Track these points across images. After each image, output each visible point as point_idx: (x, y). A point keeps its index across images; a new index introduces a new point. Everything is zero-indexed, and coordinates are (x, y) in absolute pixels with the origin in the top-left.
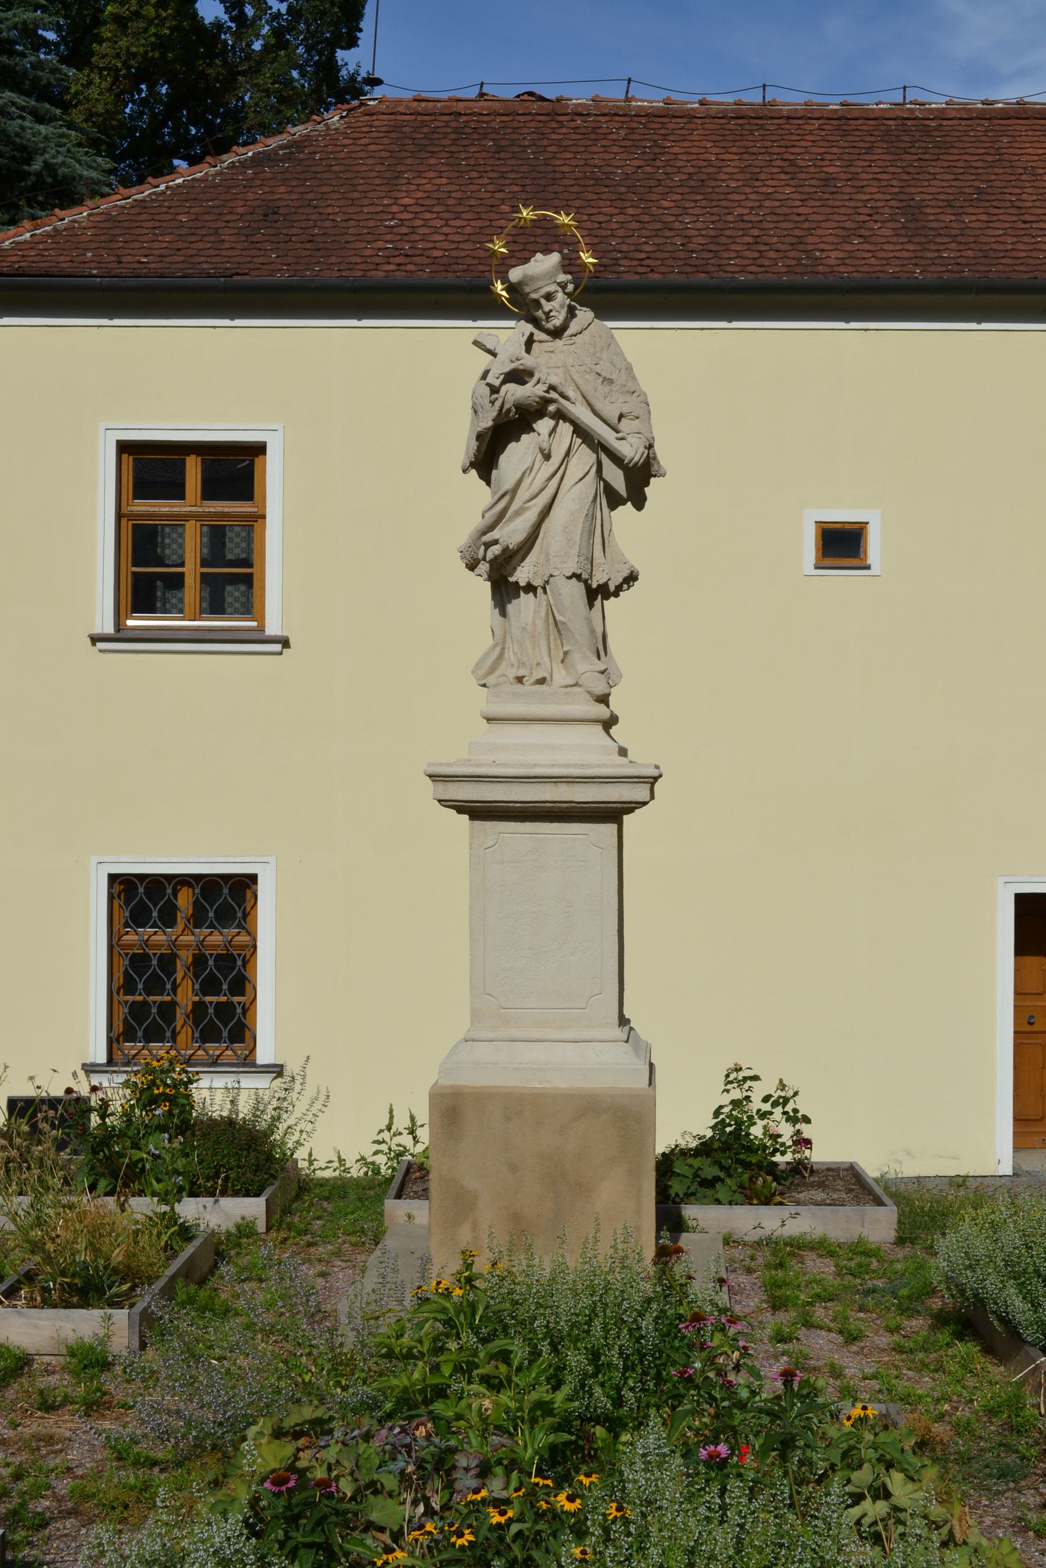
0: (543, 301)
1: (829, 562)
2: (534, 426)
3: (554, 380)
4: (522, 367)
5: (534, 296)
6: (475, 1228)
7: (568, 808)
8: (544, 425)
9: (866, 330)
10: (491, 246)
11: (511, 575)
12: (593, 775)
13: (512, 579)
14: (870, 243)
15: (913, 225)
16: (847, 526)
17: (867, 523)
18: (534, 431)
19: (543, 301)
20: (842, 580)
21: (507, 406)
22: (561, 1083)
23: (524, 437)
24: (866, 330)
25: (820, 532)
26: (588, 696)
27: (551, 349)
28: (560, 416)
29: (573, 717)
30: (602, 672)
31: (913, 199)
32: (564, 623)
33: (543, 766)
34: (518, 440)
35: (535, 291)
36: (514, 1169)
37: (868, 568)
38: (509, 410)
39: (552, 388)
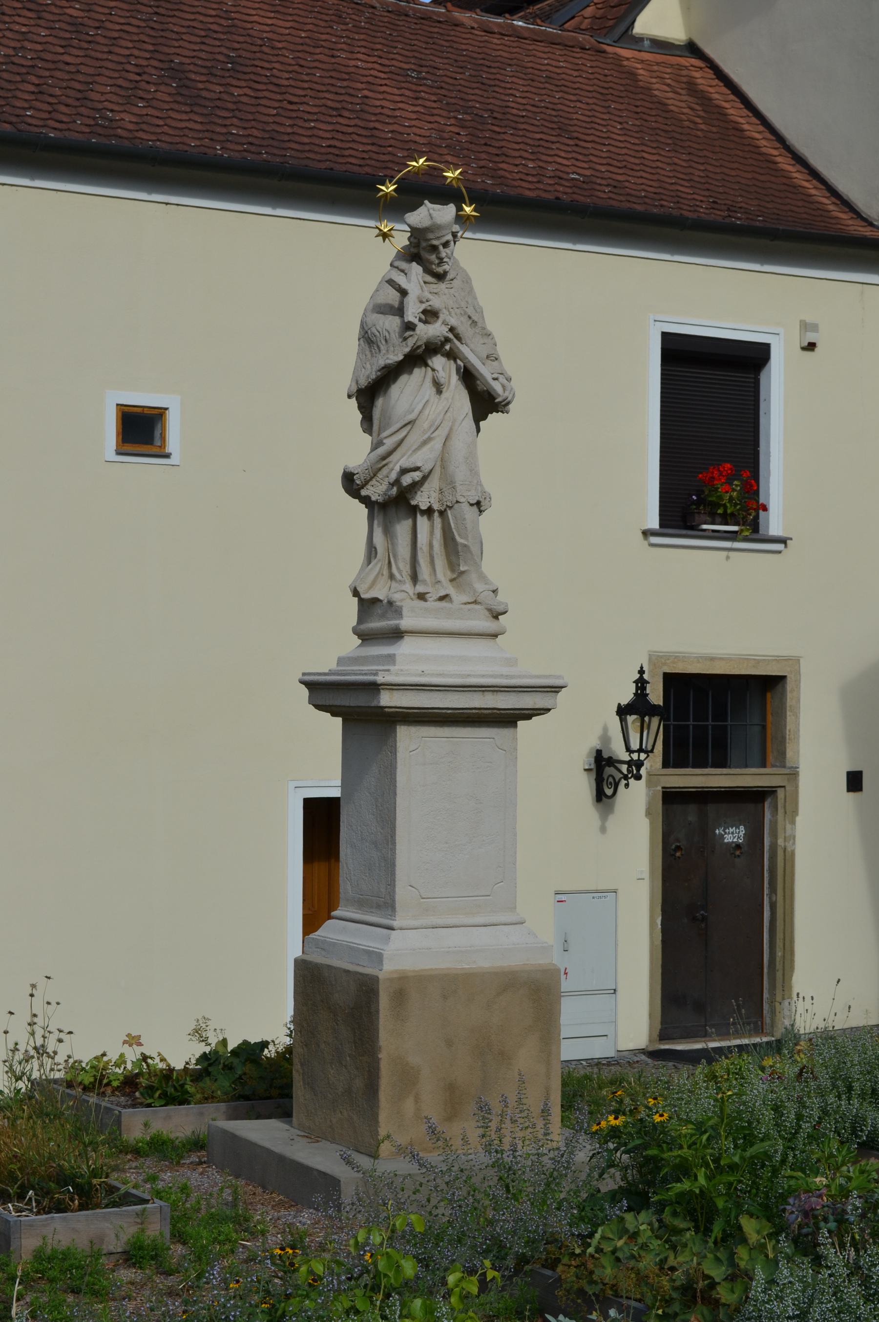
0: (441, 248)
1: (128, 448)
2: (429, 362)
3: (453, 321)
4: (429, 308)
5: (435, 242)
6: (417, 1100)
7: (489, 714)
8: (438, 362)
9: (167, 204)
10: (383, 188)
11: (413, 498)
12: (517, 685)
13: (413, 503)
14: (153, 107)
15: (184, 91)
16: (146, 411)
17: (166, 409)
18: (426, 365)
19: (441, 248)
20: (140, 468)
21: (419, 343)
22: (484, 963)
23: (417, 371)
24: (167, 204)
25: (120, 414)
26: (487, 613)
27: (435, 291)
28: (452, 355)
29: (476, 631)
30: (494, 591)
31: (172, 61)
32: (465, 546)
33: (451, 676)
34: (411, 373)
35: (438, 238)
36: (449, 1043)
37: (167, 456)
38: (419, 347)
39: (452, 330)
